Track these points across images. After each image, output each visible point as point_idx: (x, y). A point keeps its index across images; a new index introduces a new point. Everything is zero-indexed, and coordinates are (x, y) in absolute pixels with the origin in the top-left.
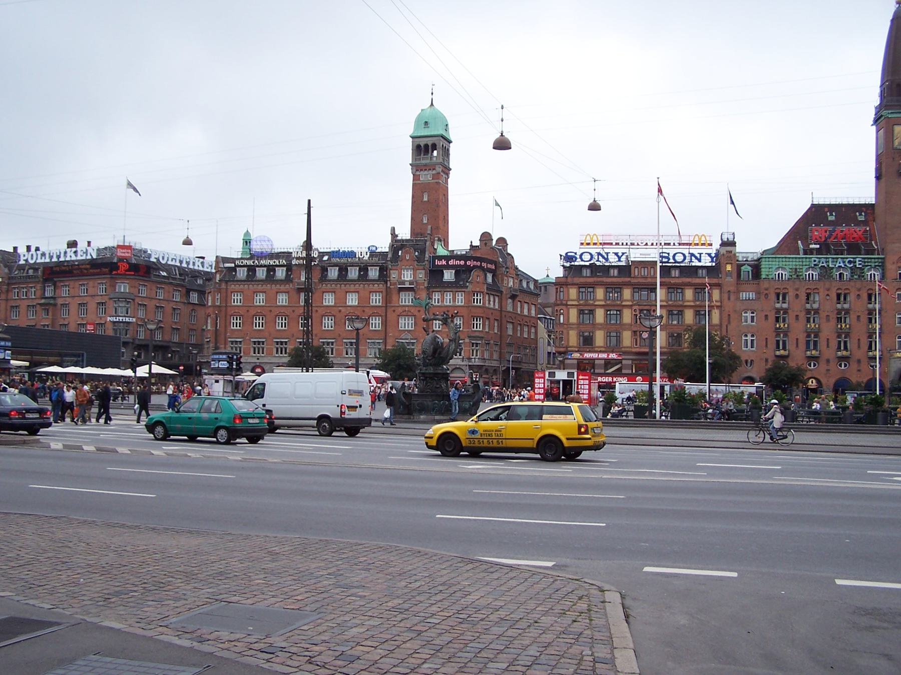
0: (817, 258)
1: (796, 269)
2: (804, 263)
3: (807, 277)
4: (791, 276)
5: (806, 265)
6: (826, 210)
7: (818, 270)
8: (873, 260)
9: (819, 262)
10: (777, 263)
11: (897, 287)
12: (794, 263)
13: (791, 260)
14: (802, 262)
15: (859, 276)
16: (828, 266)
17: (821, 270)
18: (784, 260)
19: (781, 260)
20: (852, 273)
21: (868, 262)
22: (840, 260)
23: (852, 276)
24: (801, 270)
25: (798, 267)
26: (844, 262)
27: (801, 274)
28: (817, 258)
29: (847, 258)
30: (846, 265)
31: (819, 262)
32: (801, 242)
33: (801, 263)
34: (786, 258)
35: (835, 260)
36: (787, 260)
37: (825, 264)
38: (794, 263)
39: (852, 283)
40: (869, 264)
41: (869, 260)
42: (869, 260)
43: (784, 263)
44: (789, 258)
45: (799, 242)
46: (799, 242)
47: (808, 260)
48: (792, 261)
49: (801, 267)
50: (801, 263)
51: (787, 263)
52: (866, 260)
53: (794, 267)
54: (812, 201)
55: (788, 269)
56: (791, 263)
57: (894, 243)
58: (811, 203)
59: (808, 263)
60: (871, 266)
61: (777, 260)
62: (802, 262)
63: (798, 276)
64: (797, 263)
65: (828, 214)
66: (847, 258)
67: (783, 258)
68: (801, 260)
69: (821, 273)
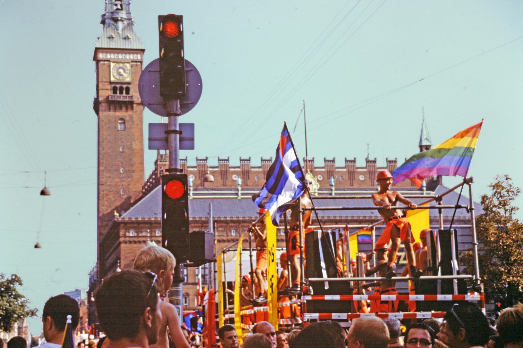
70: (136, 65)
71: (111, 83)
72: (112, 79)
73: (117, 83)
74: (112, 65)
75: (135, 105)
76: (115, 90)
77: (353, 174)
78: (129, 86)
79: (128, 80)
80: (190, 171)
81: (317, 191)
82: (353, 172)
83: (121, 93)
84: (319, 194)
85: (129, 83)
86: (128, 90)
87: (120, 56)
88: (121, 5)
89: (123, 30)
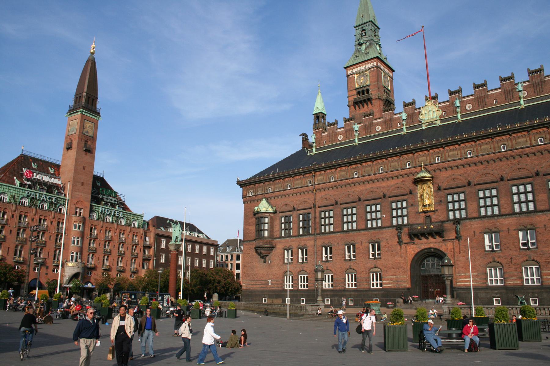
0: (30, 191)
1: (14, 196)
2: (21, 193)
3: (23, 203)
4: (10, 200)
5: (22, 195)
6: (31, 160)
7: (29, 200)
8: (63, 200)
9: (31, 194)
10: (2, 189)
11: (75, 220)
12: (14, 192)
13: (12, 189)
14: (20, 192)
15: (53, 209)
16: (36, 198)
17: (31, 200)
18: (7, 188)
19: (5, 187)
20: (49, 206)
21: (60, 201)
22: (43, 196)
23: (49, 208)
24: (18, 198)
25: (16, 195)
26: (46, 198)
27: (17, 200)
28: (30, 191)
29: (48, 195)
30: (47, 200)
31: (31, 194)
32: (16, 178)
33: (19, 193)
34: (9, 186)
35: (41, 195)
36: (10, 188)
37: (34, 197)
38: (14, 192)
39: (50, 213)
40: (60, 202)
41: (61, 200)
42: (61, 200)
43: (7, 190)
44: (11, 187)
45: (15, 178)
46: (15, 178)
47: (23, 191)
48: (13, 190)
49: (18, 195)
50: (19, 193)
51: (10, 191)
52: (59, 199)
53: (14, 194)
54: (22, 152)
55: (9, 196)
56: (12, 191)
57: (76, 191)
58: (21, 153)
59: (23, 194)
60: (61, 203)
61: (3, 187)
62: (20, 192)
63: (15, 201)
64: (16, 192)
65: (33, 164)
66: (48, 195)
67: (7, 186)
68: (19, 190)
69: (31, 202)
70: (373, 71)
71: (356, 89)
72: (357, 86)
73: (360, 88)
74: (356, 76)
75: (373, 101)
76: (359, 93)
77: (511, 93)
78: (368, 87)
79: (368, 83)
80: (339, 132)
81: (438, 118)
82: (510, 90)
83: (363, 94)
84: (442, 121)
85: (368, 86)
86: (368, 91)
87: (362, 68)
88: (365, 33)
89: (365, 49)
